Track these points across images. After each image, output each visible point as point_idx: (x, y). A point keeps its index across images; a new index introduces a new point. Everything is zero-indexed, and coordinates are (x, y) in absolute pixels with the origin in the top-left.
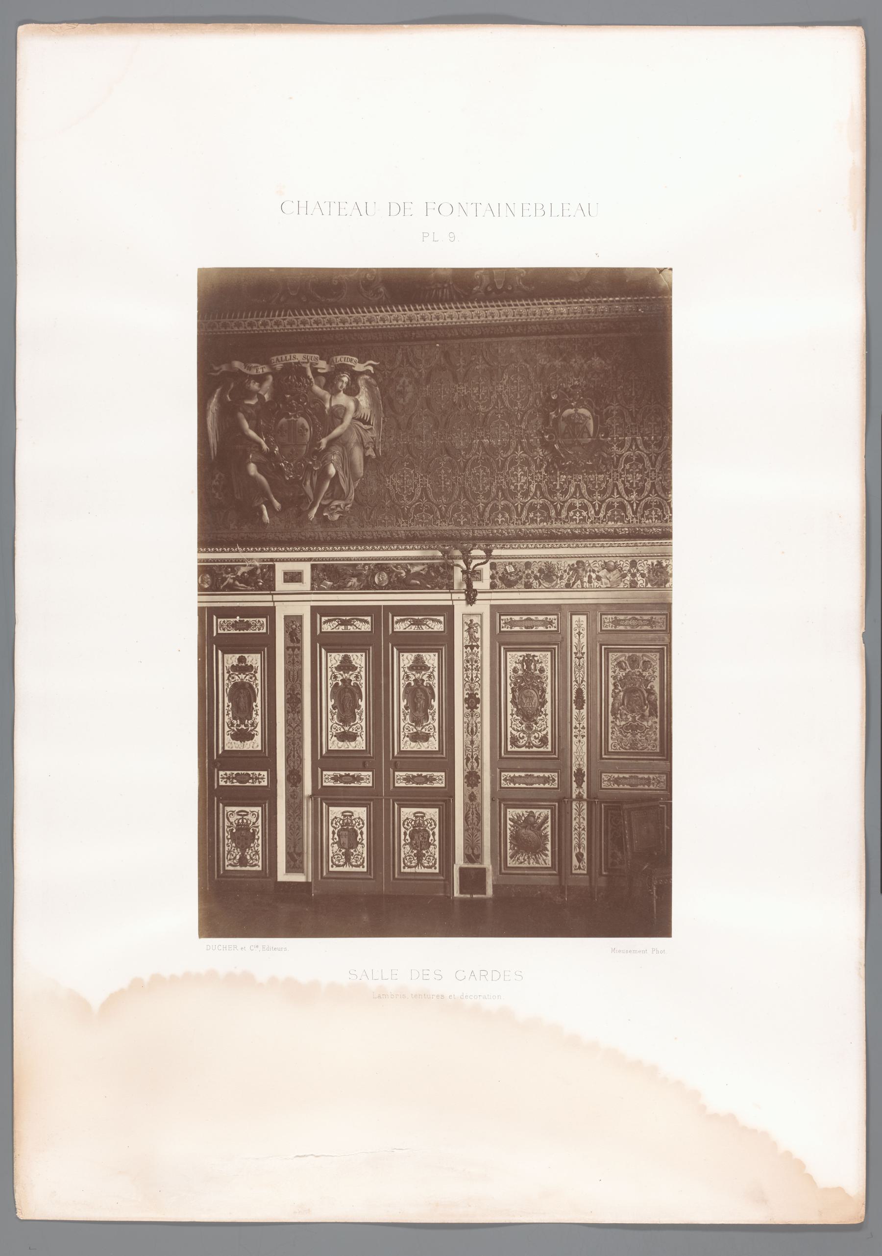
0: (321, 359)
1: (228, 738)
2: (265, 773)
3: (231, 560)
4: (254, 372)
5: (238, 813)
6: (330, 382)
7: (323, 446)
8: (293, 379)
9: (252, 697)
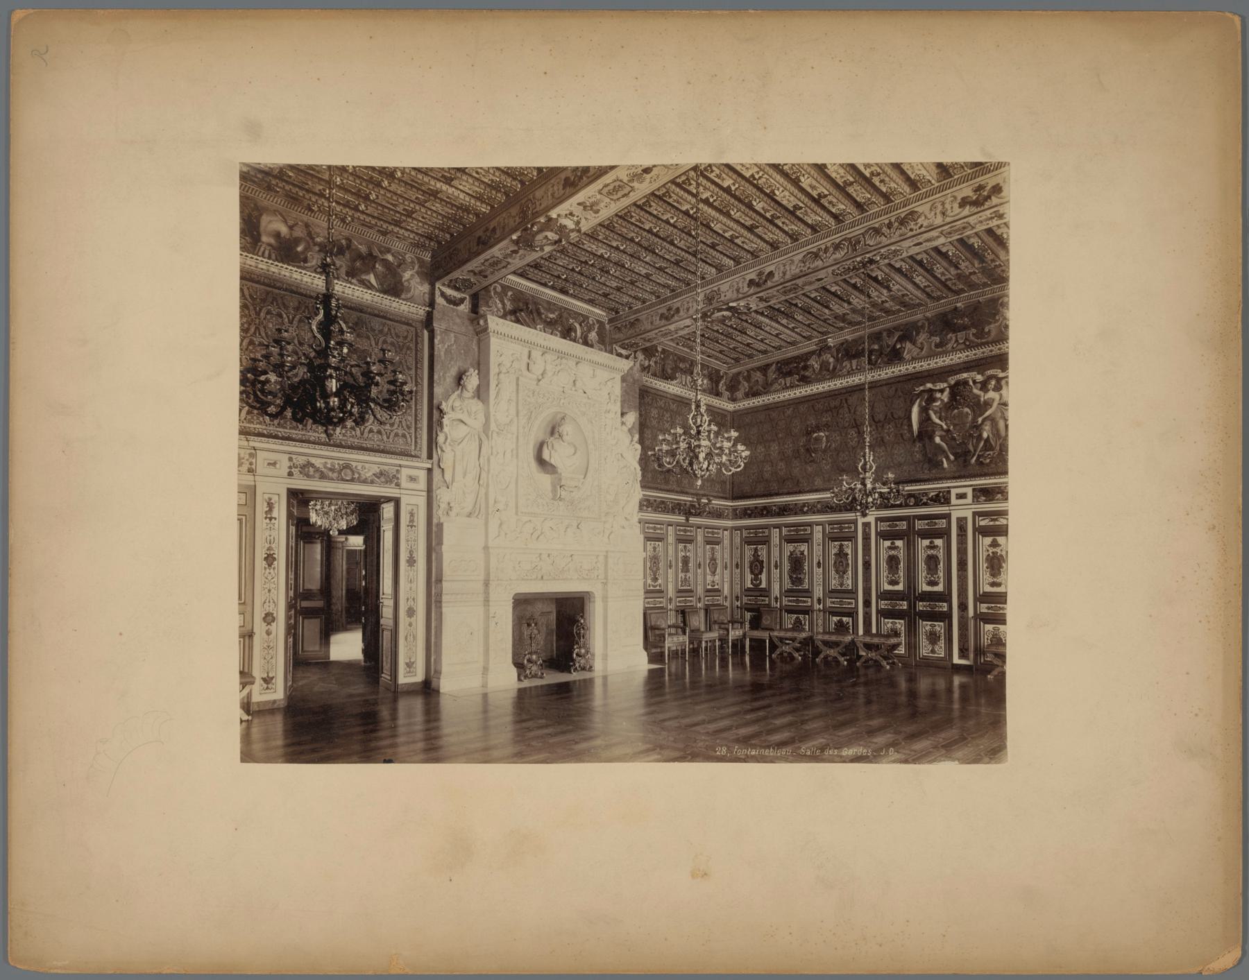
0: (978, 374)
1: (886, 584)
2: (945, 604)
3: (925, 489)
4: (938, 388)
5: (930, 625)
6: (984, 386)
7: (980, 422)
8: (961, 388)
9: (898, 563)
